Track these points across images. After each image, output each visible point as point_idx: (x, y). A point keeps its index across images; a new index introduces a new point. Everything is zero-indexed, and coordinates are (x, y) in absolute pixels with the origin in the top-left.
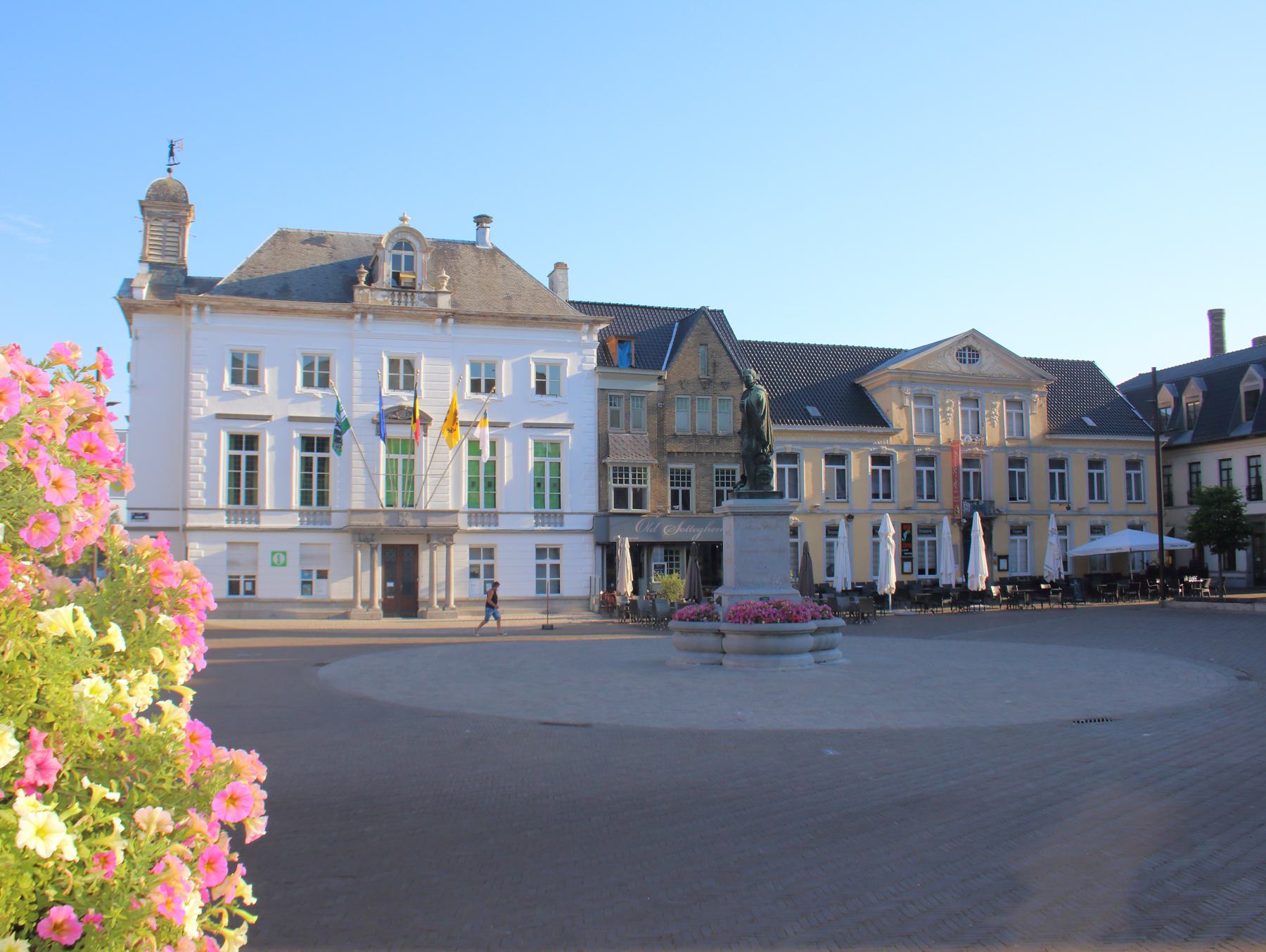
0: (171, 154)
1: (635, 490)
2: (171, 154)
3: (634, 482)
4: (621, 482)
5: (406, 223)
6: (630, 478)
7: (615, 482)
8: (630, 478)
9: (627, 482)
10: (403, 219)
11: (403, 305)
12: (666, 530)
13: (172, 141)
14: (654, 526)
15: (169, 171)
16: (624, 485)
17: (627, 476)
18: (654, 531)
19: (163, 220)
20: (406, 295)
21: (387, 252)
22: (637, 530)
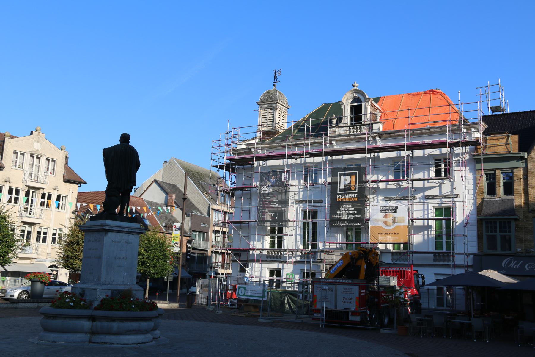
0: (275, 77)
1: (503, 238)
2: (275, 77)
3: (501, 231)
4: (491, 231)
5: (356, 87)
6: (498, 229)
7: (487, 231)
8: (498, 229)
9: (495, 231)
10: (354, 86)
11: (355, 133)
12: (528, 267)
13: (275, 71)
14: (516, 264)
15: (274, 85)
16: (493, 234)
17: (495, 227)
18: (517, 267)
19: (267, 110)
20: (357, 128)
21: (346, 106)
22: (503, 265)
